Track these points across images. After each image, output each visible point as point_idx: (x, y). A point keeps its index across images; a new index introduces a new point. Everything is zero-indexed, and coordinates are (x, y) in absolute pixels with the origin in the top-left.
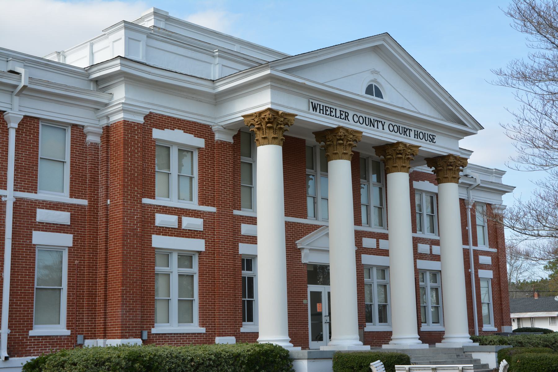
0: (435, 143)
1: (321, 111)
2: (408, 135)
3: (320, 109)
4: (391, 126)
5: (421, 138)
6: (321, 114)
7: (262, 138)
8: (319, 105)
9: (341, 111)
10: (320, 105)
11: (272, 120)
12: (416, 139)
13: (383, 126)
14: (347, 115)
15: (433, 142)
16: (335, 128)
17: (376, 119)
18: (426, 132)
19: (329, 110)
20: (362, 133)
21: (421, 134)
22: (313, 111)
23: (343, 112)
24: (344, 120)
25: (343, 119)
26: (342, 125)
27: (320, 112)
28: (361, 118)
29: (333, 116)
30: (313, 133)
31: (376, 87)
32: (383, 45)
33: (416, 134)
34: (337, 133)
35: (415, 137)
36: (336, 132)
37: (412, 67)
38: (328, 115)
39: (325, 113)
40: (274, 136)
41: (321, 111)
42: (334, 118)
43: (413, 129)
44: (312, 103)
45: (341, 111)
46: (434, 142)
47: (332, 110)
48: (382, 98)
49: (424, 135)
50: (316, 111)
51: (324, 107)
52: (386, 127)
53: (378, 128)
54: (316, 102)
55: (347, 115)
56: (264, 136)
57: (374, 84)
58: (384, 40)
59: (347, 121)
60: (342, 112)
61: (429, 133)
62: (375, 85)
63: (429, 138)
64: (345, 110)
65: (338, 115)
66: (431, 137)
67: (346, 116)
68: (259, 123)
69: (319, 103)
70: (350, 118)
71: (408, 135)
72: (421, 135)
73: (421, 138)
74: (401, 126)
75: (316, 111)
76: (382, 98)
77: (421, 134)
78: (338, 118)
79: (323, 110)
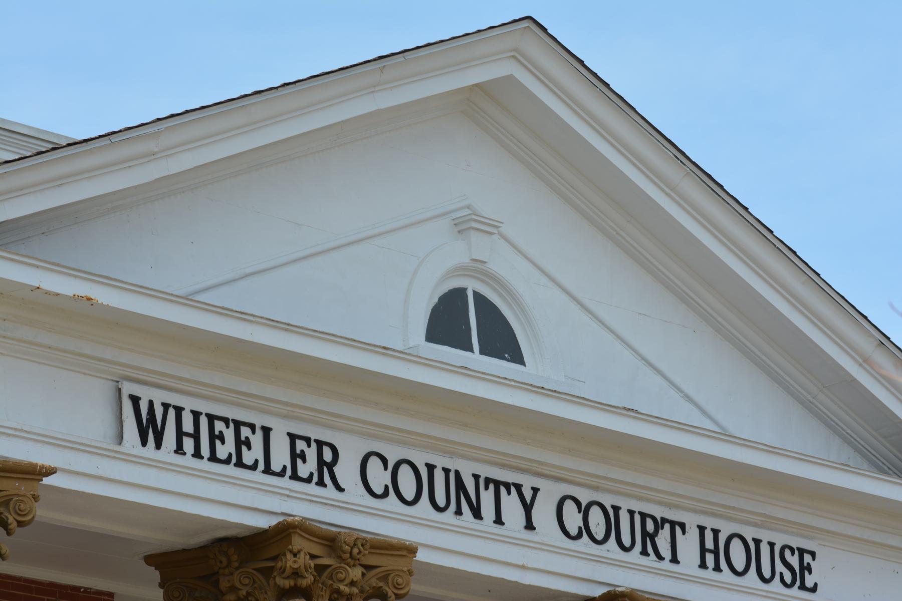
0: (814, 589)
1: (188, 444)
2: (666, 552)
3: (180, 434)
4: (569, 506)
5: (739, 565)
6: (188, 460)
8: (172, 413)
9: (293, 437)
10: (179, 410)
12: (709, 574)
13: (528, 508)
14: (328, 456)
15: (803, 587)
16: (265, 532)
17: (486, 471)
18: (766, 536)
19: (229, 435)
20: (411, 550)
21: (736, 545)
22: (144, 443)
23: (308, 440)
24: (312, 488)
25: (309, 480)
26: (301, 510)
27: (179, 450)
28: (405, 471)
29: (254, 467)
30: (150, 560)
31: (482, 302)
32: (510, 79)
33: (709, 544)
34: (275, 558)
35: (703, 565)
36: (273, 554)
37: (671, 190)
38: (227, 461)
39: (205, 450)
41: (188, 444)
42: (258, 476)
43: (692, 521)
44: (135, 400)
45: (293, 437)
46: (809, 583)
47: (245, 432)
48: (517, 358)
49: (753, 550)
50: (158, 446)
51: (204, 422)
52: (544, 513)
53: (499, 521)
54: (159, 397)
55: (328, 456)
57: (472, 286)
58: (518, 56)
59: (330, 491)
60: (301, 445)
61: (780, 541)
62: (477, 295)
63: (780, 567)
64: (315, 433)
65: (281, 457)
66: (794, 561)
67: (321, 462)
69: (175, 399)
70: (347, 471)
71: (666, 552)
72: (737, 549)
73: (739, 565)
74: (625, 505)
75: (158, 446)
76: (517, 358)
77: (736, 545)
78: (282, 474)
79: (196, 436)
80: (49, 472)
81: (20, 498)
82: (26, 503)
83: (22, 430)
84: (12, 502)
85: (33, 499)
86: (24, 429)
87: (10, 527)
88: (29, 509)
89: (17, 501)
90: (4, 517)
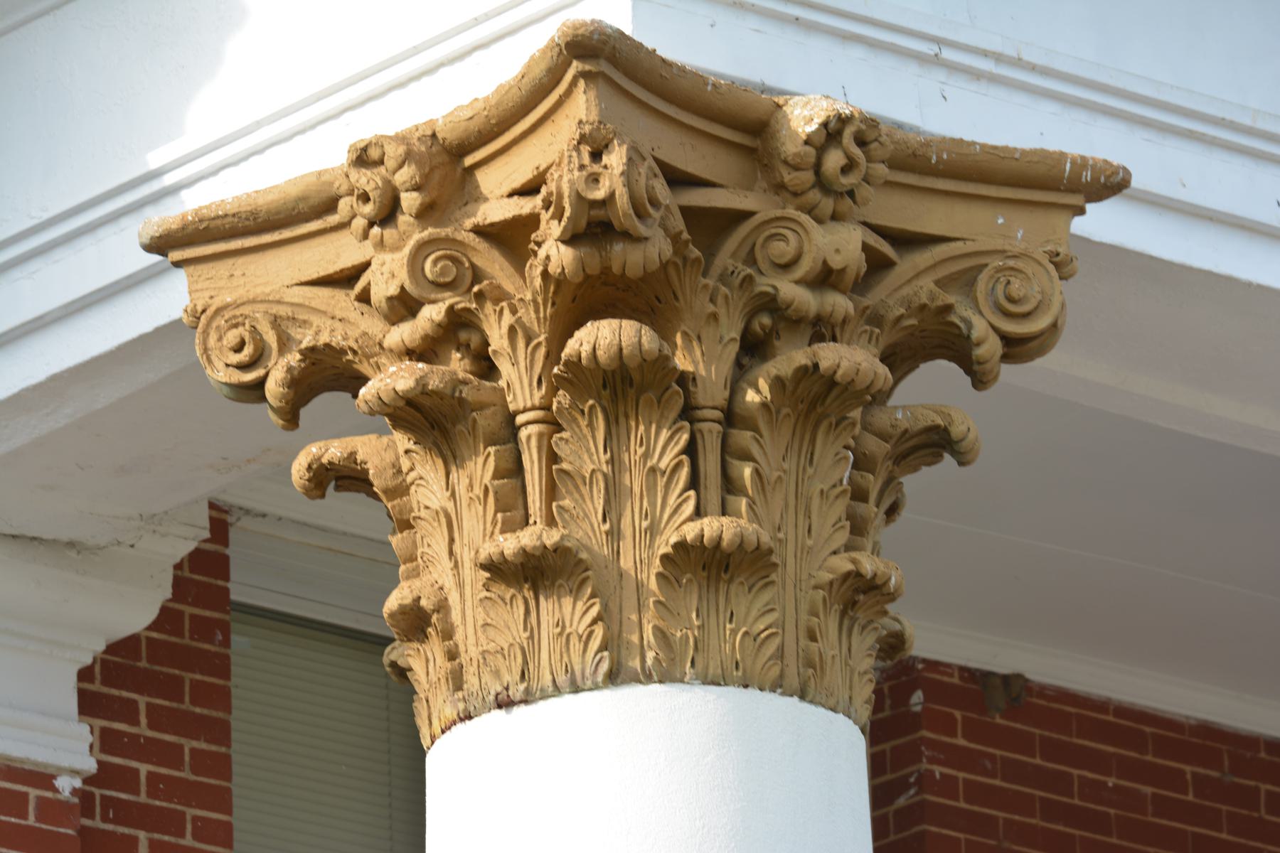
7: (497, 570)
11: (658, 248)
40: (710, 526)
56: (527, 538)
68: (432, 313)
80: (1102, 180)
81: (1011, 263)
82: (1029, 278)
83: (1018, 63)
84: (983, 279)
85: (1051, 267)
86: (1026, 57)
87: (979, 352)
88: (1039, 297)
89: (999, 270)
90: (957, 321)
